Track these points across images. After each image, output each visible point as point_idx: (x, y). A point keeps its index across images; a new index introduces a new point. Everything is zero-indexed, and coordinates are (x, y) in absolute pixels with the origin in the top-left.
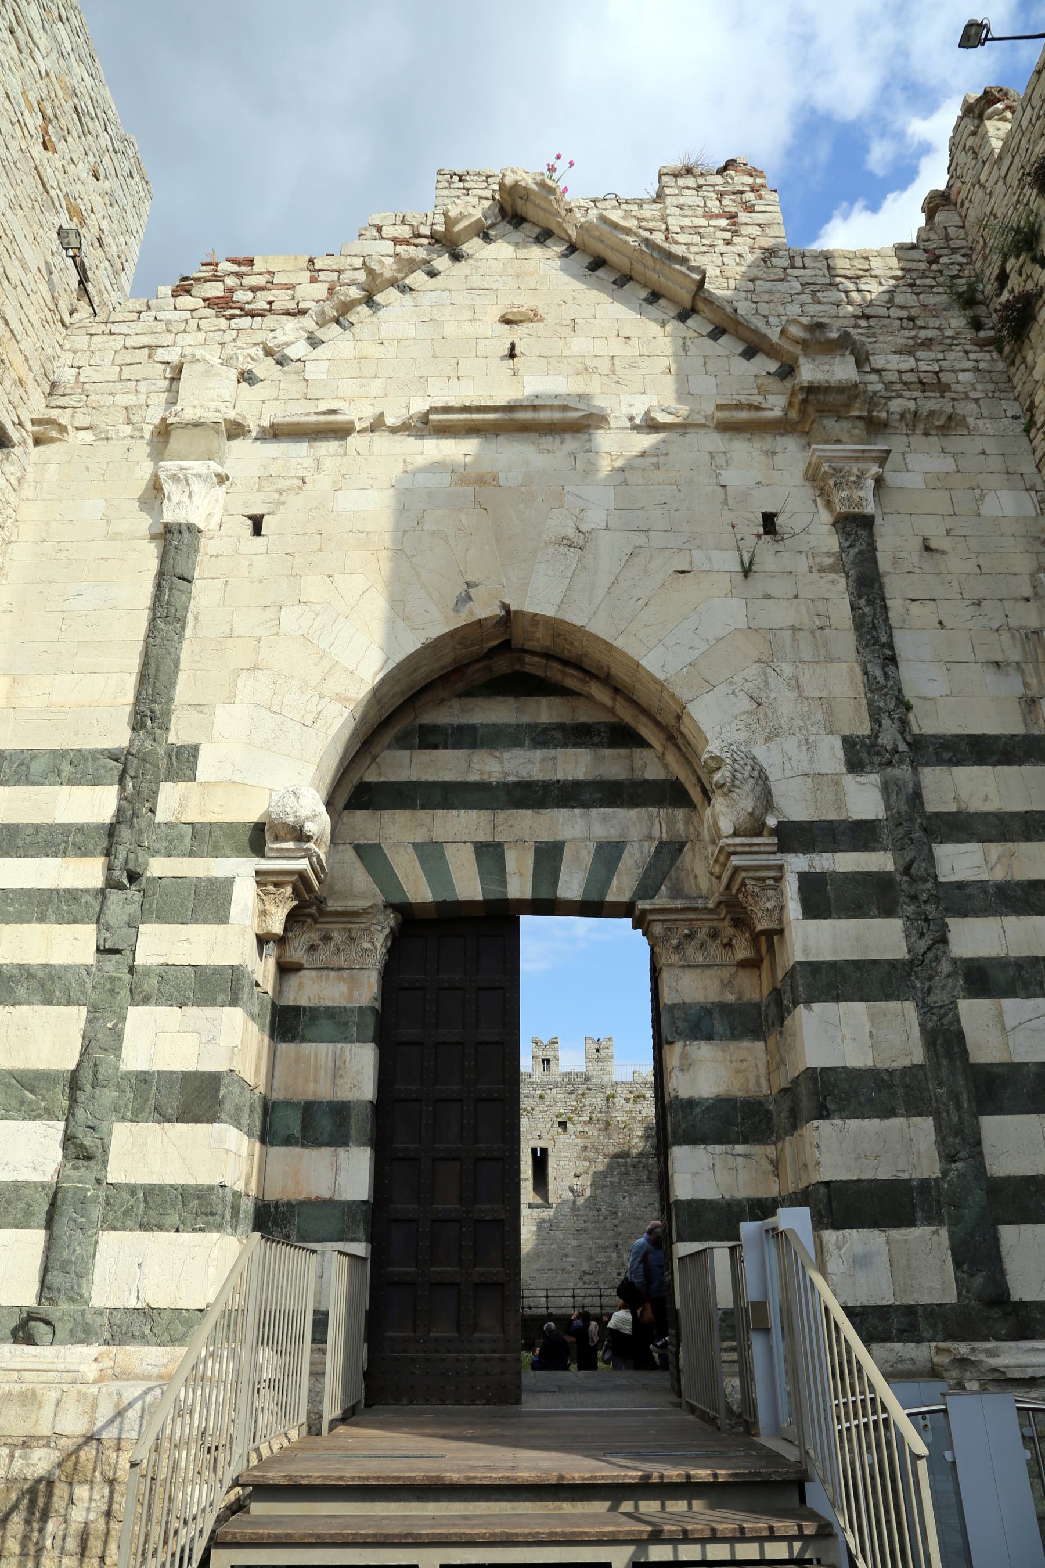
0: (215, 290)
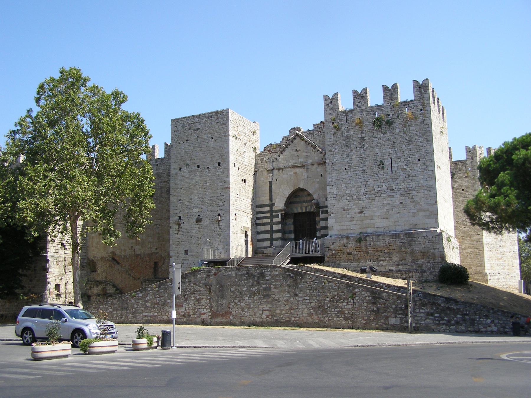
0: (268, 149)
